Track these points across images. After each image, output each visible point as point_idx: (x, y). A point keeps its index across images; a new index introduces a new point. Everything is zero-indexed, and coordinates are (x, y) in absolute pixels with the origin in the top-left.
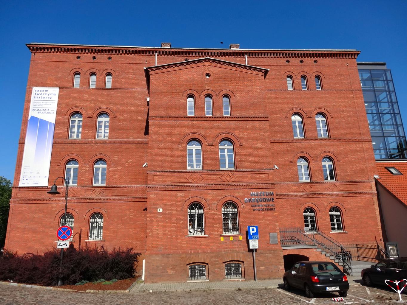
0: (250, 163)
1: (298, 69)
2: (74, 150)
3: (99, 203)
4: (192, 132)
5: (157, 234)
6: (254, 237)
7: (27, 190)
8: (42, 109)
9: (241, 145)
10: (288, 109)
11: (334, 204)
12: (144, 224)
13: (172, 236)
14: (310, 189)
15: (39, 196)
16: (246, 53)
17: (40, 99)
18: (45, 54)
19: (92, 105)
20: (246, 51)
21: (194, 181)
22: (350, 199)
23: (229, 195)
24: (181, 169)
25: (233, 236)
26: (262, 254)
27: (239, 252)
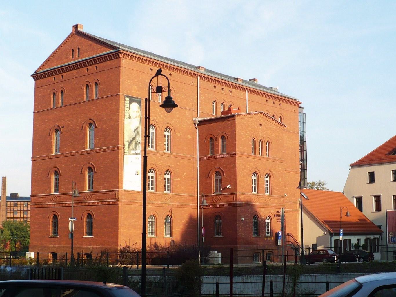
9: (273, 178)
15: (135, 198)
20: (248, 88)
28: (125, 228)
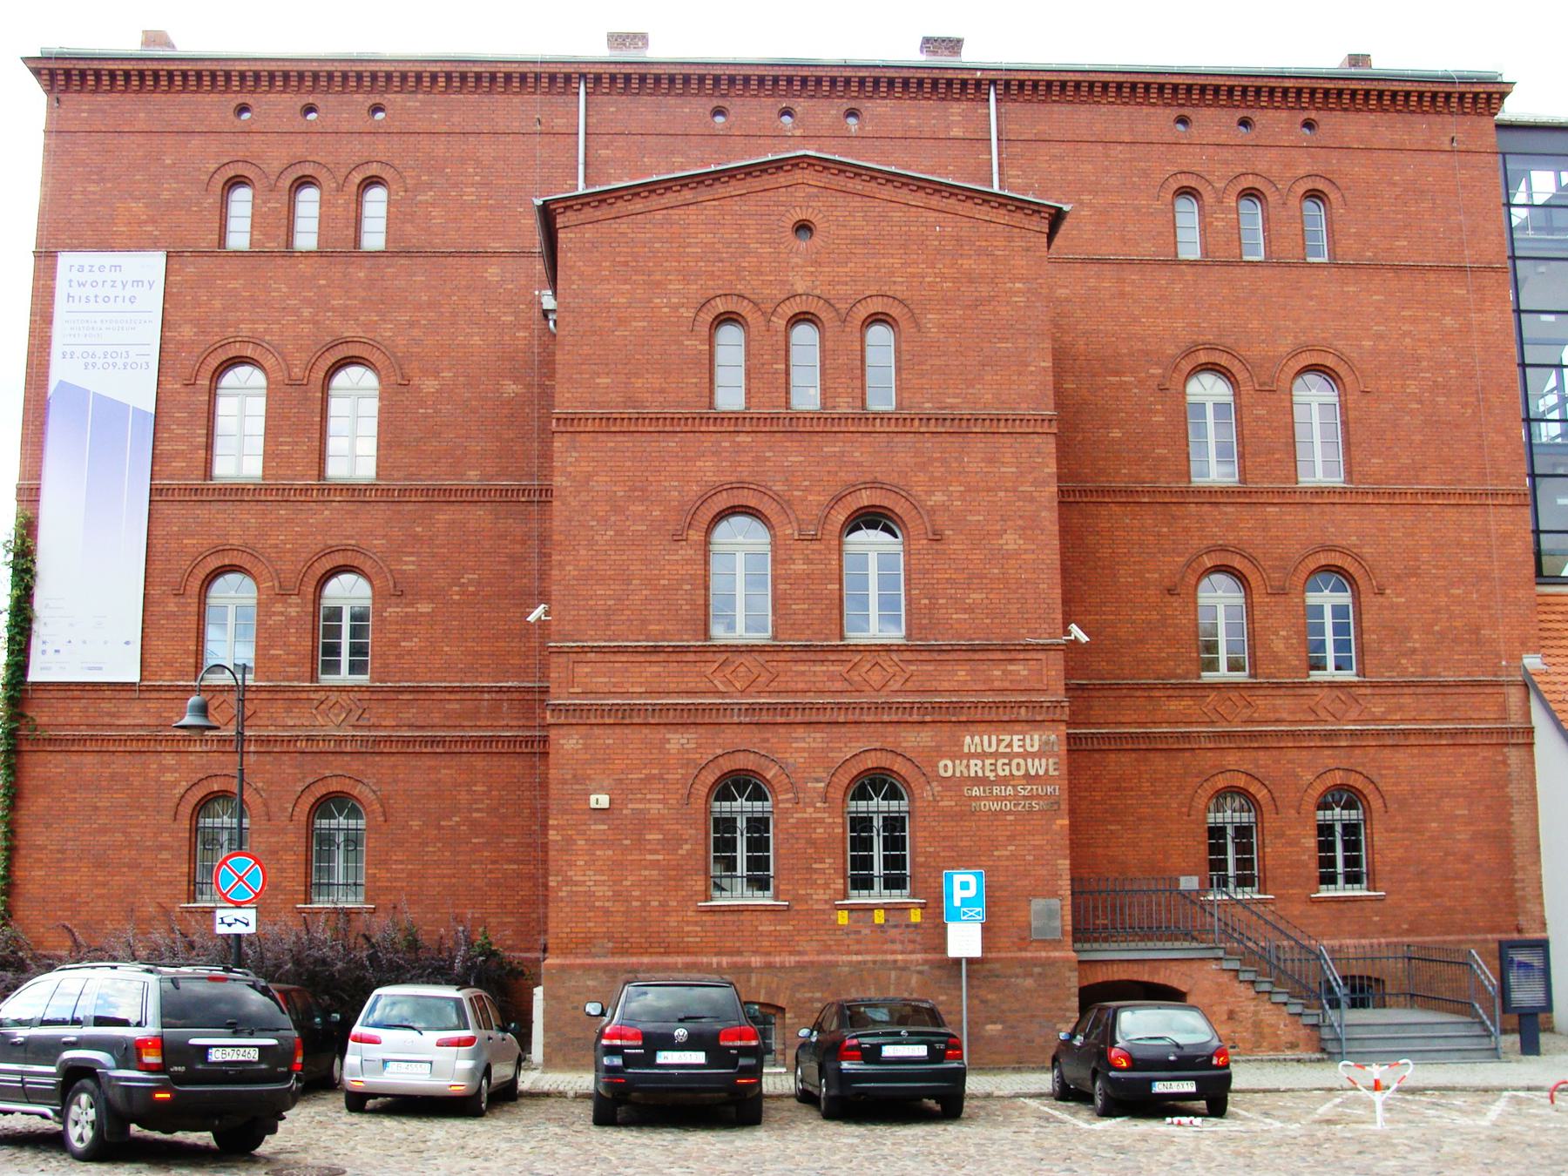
0: (966, 616)
1: (1226, 163)
2: (238, 525)
3: (347, 758)
4: (733, 479)
5: (590, 894)
6: (965, 914)
7: (62, 694)
8: (99, 351)
9: (937, 537)
10: (1171, 350)
11: (1338, 778)
12: (529, 845)
13: (646, 903)
14: (1246, 713)
15: (107, 720)
16: (993, 82)
17: (92, 306)
18: (100, 98)
19: (306, 328)
20: (992, 75)
21: (738, 685)
22: (1412, 756)
23: (878, 745)
24: (685, 637)
25: (888, 908)
26: (997, 976)
27: (904, 969)
28: (41, 860)
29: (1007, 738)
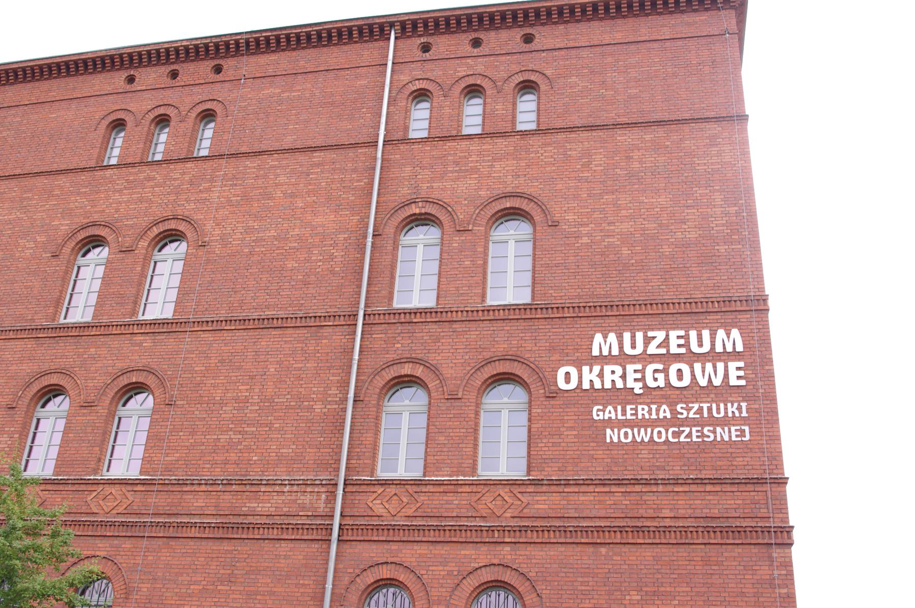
29: (660, 335)
